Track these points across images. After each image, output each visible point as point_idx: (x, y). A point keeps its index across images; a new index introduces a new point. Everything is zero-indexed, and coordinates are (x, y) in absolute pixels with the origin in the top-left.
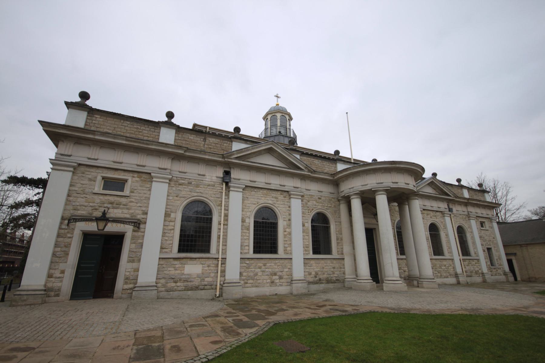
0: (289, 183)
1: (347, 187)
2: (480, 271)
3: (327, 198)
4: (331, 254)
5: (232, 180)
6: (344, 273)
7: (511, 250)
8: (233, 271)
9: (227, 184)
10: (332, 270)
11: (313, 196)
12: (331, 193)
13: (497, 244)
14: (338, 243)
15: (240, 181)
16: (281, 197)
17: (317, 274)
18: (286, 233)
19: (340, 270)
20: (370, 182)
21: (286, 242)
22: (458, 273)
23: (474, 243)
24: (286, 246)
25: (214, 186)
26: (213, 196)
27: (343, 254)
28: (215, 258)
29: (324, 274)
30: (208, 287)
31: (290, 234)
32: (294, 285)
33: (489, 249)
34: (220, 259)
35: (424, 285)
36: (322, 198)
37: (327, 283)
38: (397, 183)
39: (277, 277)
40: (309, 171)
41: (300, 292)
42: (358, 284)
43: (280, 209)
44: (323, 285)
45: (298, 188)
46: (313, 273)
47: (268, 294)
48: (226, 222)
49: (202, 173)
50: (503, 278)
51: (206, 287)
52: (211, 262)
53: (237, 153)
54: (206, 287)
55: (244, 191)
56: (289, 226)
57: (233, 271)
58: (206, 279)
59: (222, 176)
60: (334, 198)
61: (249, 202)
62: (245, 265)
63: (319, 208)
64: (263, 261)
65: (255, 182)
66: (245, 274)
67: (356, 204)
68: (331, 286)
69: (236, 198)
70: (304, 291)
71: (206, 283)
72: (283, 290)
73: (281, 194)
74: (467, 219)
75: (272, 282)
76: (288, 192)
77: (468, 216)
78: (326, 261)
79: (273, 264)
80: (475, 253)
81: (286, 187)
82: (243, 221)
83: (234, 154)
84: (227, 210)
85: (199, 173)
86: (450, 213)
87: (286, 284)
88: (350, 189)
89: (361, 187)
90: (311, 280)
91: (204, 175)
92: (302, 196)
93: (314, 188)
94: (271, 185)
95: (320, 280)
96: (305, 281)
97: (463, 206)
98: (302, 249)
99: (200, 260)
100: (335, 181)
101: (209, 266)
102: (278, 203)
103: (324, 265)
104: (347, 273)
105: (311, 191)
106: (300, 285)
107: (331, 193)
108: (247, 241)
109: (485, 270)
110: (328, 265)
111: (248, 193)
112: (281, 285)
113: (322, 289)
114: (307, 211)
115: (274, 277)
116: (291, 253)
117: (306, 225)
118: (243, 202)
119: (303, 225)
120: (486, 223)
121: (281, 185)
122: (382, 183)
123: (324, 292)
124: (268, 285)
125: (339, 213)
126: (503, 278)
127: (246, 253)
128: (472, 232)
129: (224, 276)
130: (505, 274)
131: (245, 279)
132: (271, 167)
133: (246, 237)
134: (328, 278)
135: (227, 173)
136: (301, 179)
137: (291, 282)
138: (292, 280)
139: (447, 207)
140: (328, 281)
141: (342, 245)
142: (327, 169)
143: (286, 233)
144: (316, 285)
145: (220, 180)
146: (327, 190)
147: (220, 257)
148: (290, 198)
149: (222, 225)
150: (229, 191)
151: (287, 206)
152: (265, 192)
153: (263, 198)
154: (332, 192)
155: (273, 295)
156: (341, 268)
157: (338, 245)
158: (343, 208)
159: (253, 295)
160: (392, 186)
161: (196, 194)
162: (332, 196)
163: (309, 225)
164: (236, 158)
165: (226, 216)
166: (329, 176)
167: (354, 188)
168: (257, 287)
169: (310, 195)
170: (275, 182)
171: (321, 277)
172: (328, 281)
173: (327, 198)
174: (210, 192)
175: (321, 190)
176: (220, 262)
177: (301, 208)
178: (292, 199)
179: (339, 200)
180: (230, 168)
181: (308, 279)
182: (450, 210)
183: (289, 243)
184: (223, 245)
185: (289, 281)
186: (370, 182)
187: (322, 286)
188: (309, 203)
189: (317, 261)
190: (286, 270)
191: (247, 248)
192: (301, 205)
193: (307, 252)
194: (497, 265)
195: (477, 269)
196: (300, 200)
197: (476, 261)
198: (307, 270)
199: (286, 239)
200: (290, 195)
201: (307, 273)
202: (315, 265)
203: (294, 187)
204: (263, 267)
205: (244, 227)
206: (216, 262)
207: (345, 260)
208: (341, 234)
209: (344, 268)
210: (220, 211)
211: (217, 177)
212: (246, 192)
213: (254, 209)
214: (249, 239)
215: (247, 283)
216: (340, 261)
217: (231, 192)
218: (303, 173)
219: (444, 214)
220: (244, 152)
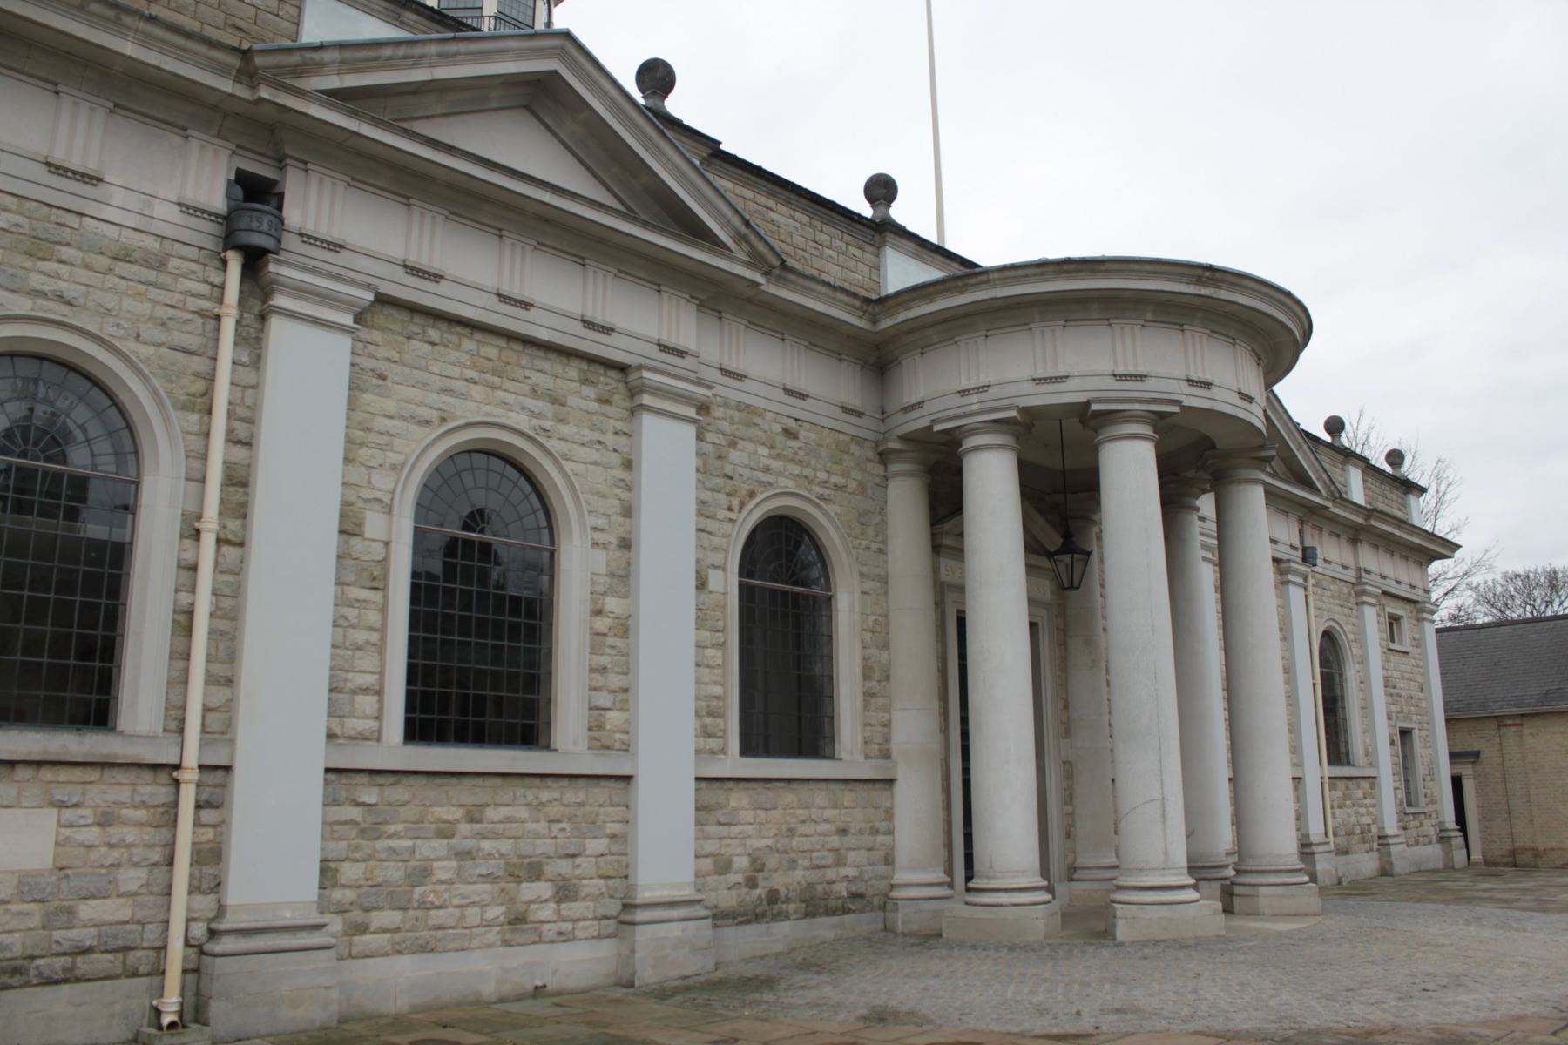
0: (640, 320)
1: (940, 386)
2: (1374, 829)
3: (829, 438)
4: (832, 757)
5: (291, 242)
6: (889, 860)
7: (1471, 743)
8: (276, 849)
9: (254, 260)
10: (834, 841)
11: (759, 412)
12: (846, 410)
13: (1428, 713)
14: (869, 694)
15: (343, 258)
16: (582, 398)
17: (757, 865)
18: (602, 624)
19: (867, 840)
20: (1084, 365)
21: (599, 680)
22: (1314, 839)
23: (1367, 708)
24: (603, 699)
25: (160, 264)
26: (151, 332)
27: (886, 756)
28: (155, 767)
29: (793, 865)
30: (102, 962)
31: (625, 628)
32: (643, 935)
33: (1405, 733)
34: (190, 775)
36: (803, 434)
37: (807, 915)
38: (1207, 385)
39: (544, 889)
40: (756, 260)
41: (674, 973)
42: (981, 913)
43: (573, 470)
45: (682, 353)
46: (741, 862)
47: (488, 989)
48: (233, 525)
49: (75, 163)
50: (1432, 854)
51: (83, 965)
52: (123, 794)
53: (344, 67)
54: (83, 965)
55: (364, 333)
56: (623, 578)
57: (276, 849)
58: (86, 910)
59: (219, 203)
60: (859, 441)
61: (390, 406)
62: (355, 813)
64: (466, 793)
65: (436, 277)
66: (350, 872)
67: (993, 484)
68: (824, 929)
69: (307, 366)
70: (694, 965)
71: (87, 936)
72: (577, 961)
73: (585, 381)
74: (1353, 600)
75: (518, 920)
76: (623, 369)
77: (1358, 589)
78: (805, 792)
79: (523, 813)
80: (1367, 754)
81: (615, 339)
82: (349, 528)
83: (319, 68)
84: (244, 439)
85: (59, 156)
86: (1305, 569)
87: (594, 928)
88: (964, 393)
89: (1030, 387)
90: (728, 899)
91: (94, 180)
92: (703, 408)
93: (765, 366)
94: (532, 314)
95: (773, 897)
96: (700, 911)
97: (1343, 542)
98: (690, 724)
99: (47, 774)
100: (877, 346)
101: (106, 820)
102: (565, 430)
103: (797, 820)
104: (901, 857)
105: (748, 385)
106: (675, 930)
107: (846, 410)
108: (368, 661)
109: (1391, 826)
110: (815, 813)
111: (384, 340)
112: (565, 937)
113: (780, 947)
114: (721, 497)
115: (529, 890)
116: (626, 748)
117: (715, 580)
118: (352, 405)
119: (701, 585)
120: (1405, 623)
121: (588, 324)
122: (1140, 378)
123: (812, 963)
124: (493, 935)
125: (882, 528)
126: (1432, 854)
127: (362, 737)
128: (1363, 661)
129: (217, 886)
130: (1443, 839)
131: (351, 904)
132: (547, 197)
133: (360, 636)
134: (810, 885)
135: (255, 192)
136: (701, 306)
137: (626, 914)
138: (628, 907)
139: (1297, 543)
140: (815, 905)
141: (888, 709)
142: (834, 269)
143: (602, 624)
144: (750, 929)
145: (205, 234)
146: (829, 386)
147: (191, 759)
148: (635, 411)
149: (208, 541)
150: (263, 318)
151: (616, 459)
152: (491, 351)
153: (477, 392)
154: (855, 402)
155: (520, 998)
156: (875, 831)
157: (866, 708)
158: (905, 502)
159: (402, 1004)
160: (1187, 402)
161: (23, 306)
162: (850, 426)
163: (727, 584)
164: (341, 98)
165: (238, 480)
167: (993, 393)
168: (424, 949)
169: (740, 407)
170: (559, 295)
172: (815, 905)
173: (829, 438)
174: (128, 304)
175: (801, 385)
176: (188, 796)
177: (692, 477)
178: (648, 421)
179: (884, 457)
180: (280, 162)
181: (710, 898)
182: (1308, 556)
183: (616, 681)
184: (211, 680)
185: (614, 907)
186: (1084, 365)
187: (783, 933)
188: (734, 455)
189: (764, 794)
190: (596, 845)
191: (367, 703)
192: (692, 462)
193: (712, 743)
194: (1423, 801)
195: (1366, 820)
196: (691, 431)
197: (1365, 784)
198: (711, 846)
199: (604, 660)
200: (633, 392)
201: (708, 863)
202: (747, 815)
203: (664, 348)
204: (464, 828)
205: (357, 572)
206: (162, 793)
207: (898, 786)
208: (886, 646)
209: (890, 832)
210: (196, 443)
211: (185, 208)
212: (376, 336)
213: (418, 452)
214: (381, 648)
215: (362, 929)
216: (876, 793)
217: (276, 324)
218: (722, 263)
219: (1288, 571)
220: (388, 64)
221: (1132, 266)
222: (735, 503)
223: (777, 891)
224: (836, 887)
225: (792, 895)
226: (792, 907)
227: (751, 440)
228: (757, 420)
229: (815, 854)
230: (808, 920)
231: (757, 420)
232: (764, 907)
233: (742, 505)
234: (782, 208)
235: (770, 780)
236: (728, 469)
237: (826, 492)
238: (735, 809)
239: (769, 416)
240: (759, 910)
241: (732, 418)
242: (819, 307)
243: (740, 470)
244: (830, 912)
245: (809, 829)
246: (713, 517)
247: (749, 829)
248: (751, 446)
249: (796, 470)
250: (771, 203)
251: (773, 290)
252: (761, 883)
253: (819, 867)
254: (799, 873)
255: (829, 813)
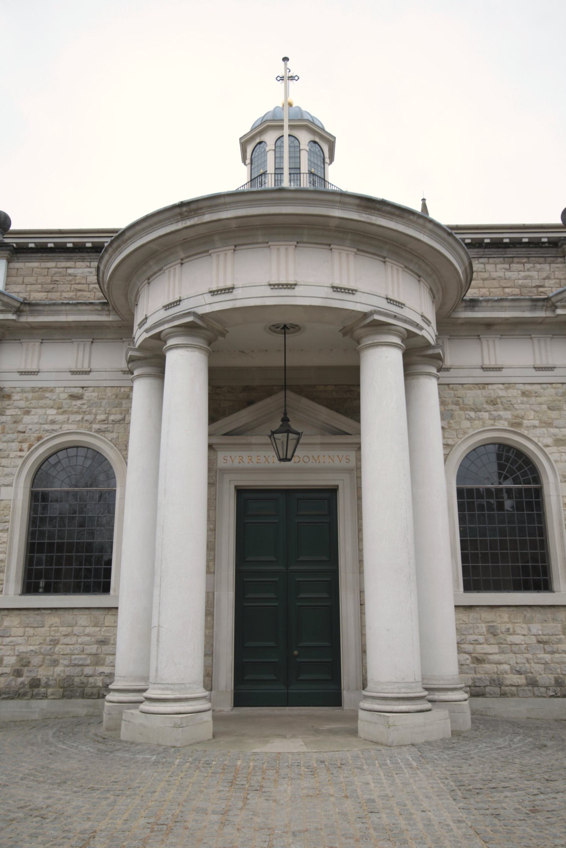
3: (109, 392)
10: (93, 649)
11: (52, 390)
29: (55, 663)
35: (361, 725)
37: (63, 697)
44: (44, 704)
63: (71, 429)
78: (68, 617)
95: (35, 683)
110: (76, 630)
134: (69, 677)
144: (11, 703)
166: (98, 312)
169: (33, 390)
171: (42, 674)
188: (27, 419)
189: (32, 618)
202: (20, 631)
221: (138, 228)
222: (25, 446)
223: (39, 680)
224: (91, 680)
225: (51, 683)
226: (50, 691)
227: (42, 407)
228: (48, 395)
229: (74, 657)
230: (65, 700)
231: (48, 395)
232: (27, 689)
233: (31, 446)
234: (79, 264)
235: (56, 609)
236: (21, 427)
237: (103, 427)
238: (9, 628)
239: (58, 390)
240: (22, 691)
241: (27, 398)
242: (71, 318)
243: (30, 427)
244: (83, 696)
245: (67, 640)
246: (8, 457)
247: (20, 640)
248: (40, 411)
249: (79, 417)
250: (69, 264)
251: (31, 319)
252: (26, 673)
253: (75, 665)
254: (58, 669)
255: (88, 630)
